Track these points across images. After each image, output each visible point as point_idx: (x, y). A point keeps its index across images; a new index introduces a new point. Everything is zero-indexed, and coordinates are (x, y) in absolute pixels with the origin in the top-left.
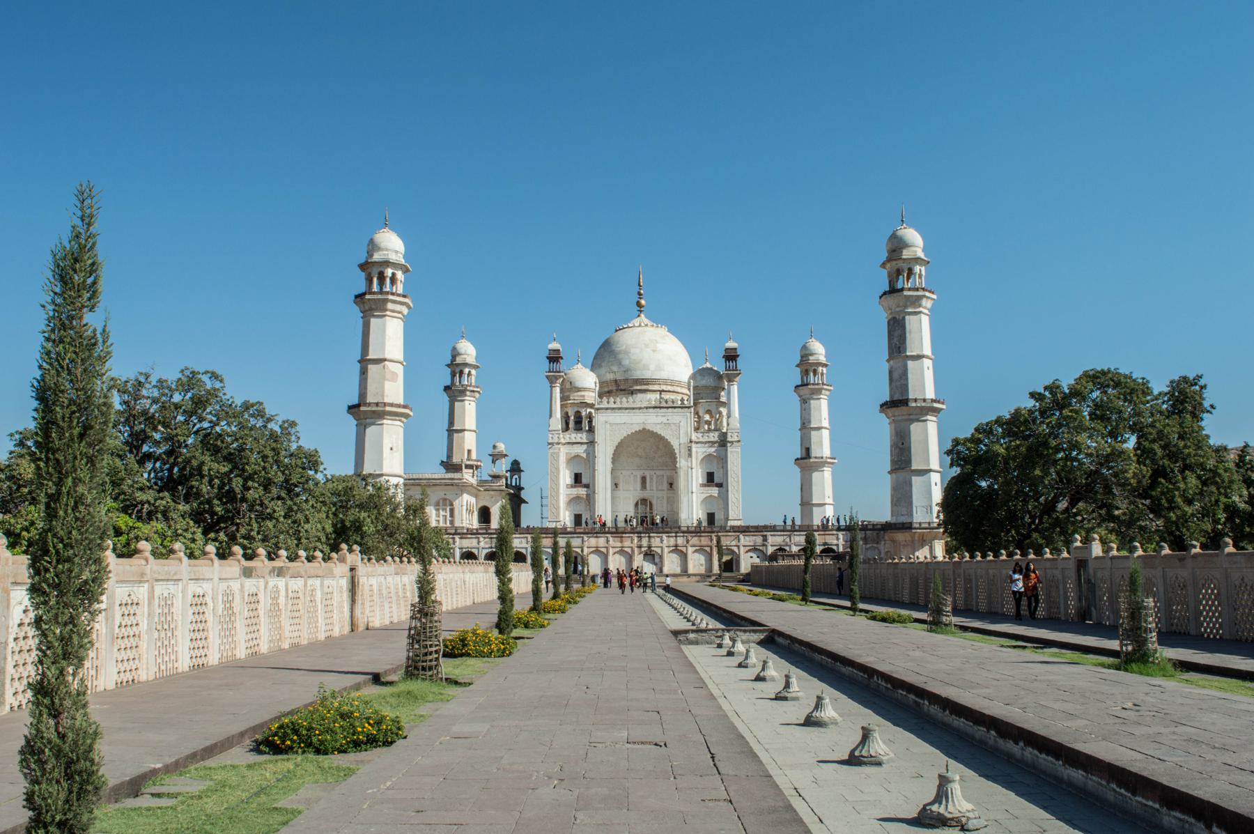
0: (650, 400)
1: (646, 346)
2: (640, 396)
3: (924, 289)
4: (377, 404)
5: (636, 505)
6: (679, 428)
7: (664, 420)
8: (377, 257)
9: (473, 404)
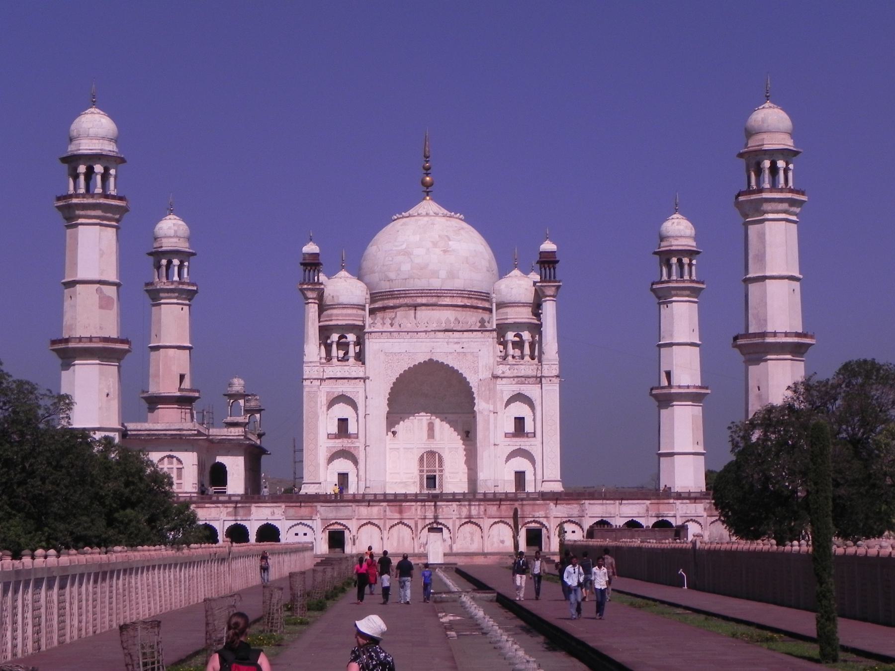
0: (439, 322)
1: (435, 244)
2: (423, 313)
3: (791, 191)
4: (91, 339)
5: (421, 459)
6: (475, 358)
7: (458, 348)
8: (86, 146)
9: (186, 308)
